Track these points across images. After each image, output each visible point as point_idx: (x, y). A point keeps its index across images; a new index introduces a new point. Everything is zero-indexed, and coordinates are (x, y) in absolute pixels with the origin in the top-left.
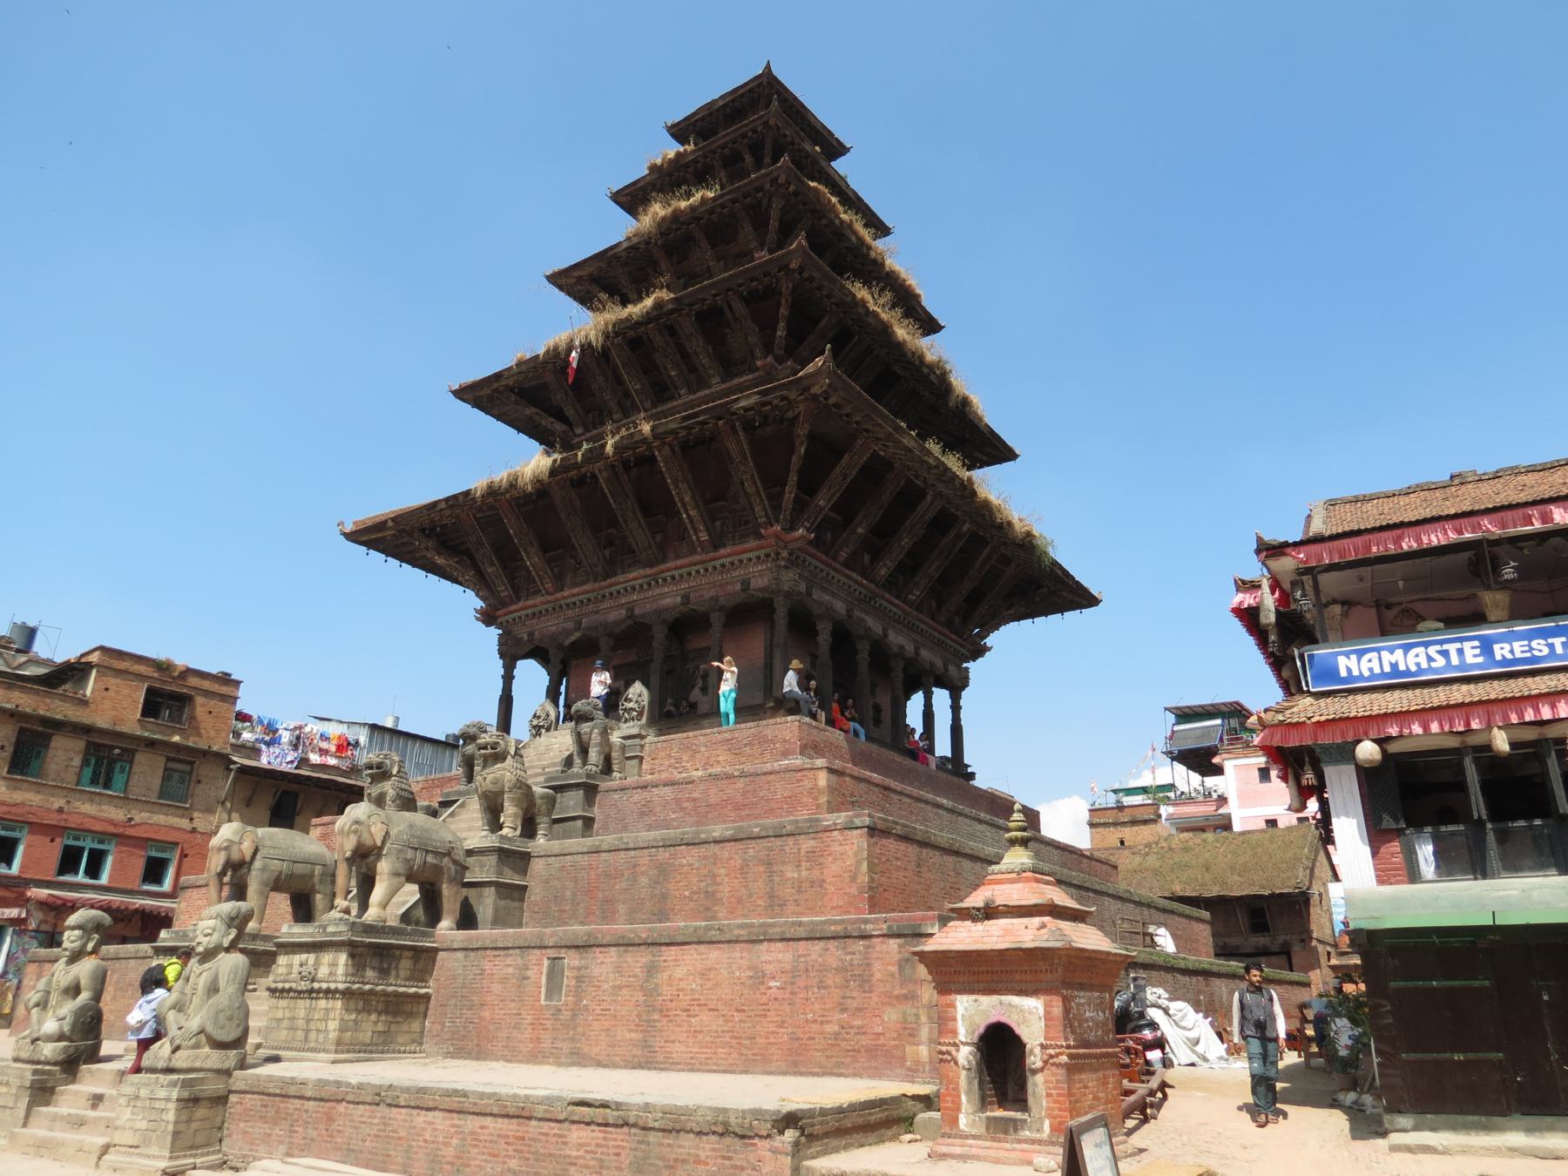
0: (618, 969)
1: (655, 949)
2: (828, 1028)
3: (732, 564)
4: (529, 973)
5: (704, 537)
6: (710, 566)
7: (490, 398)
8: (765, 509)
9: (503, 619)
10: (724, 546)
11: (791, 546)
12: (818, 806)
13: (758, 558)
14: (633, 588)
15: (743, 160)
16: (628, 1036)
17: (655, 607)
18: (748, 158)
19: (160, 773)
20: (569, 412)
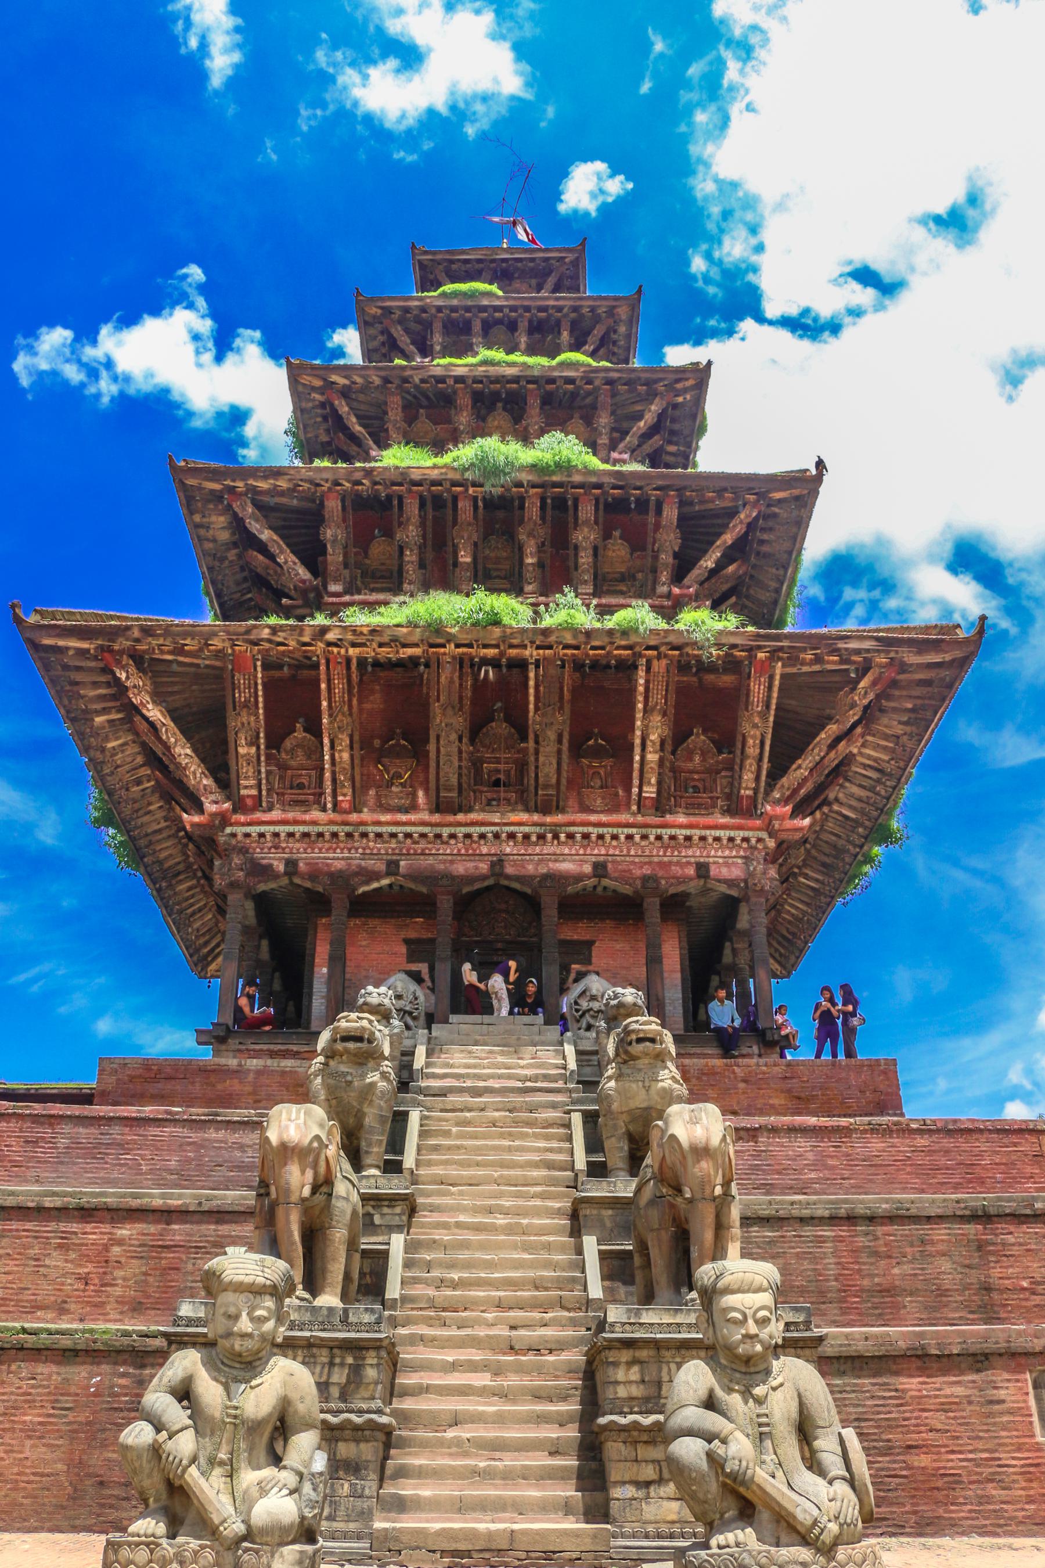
3: (688, 838)
4: (1002, 1394)
5: (650, 792)
6: (652, 833)
8: (757, 779)
11: (784, 836)
13: (731, 839)
14: (512, 836)
17: (545, 871)
18: (565, 335)
20: (334, 557)
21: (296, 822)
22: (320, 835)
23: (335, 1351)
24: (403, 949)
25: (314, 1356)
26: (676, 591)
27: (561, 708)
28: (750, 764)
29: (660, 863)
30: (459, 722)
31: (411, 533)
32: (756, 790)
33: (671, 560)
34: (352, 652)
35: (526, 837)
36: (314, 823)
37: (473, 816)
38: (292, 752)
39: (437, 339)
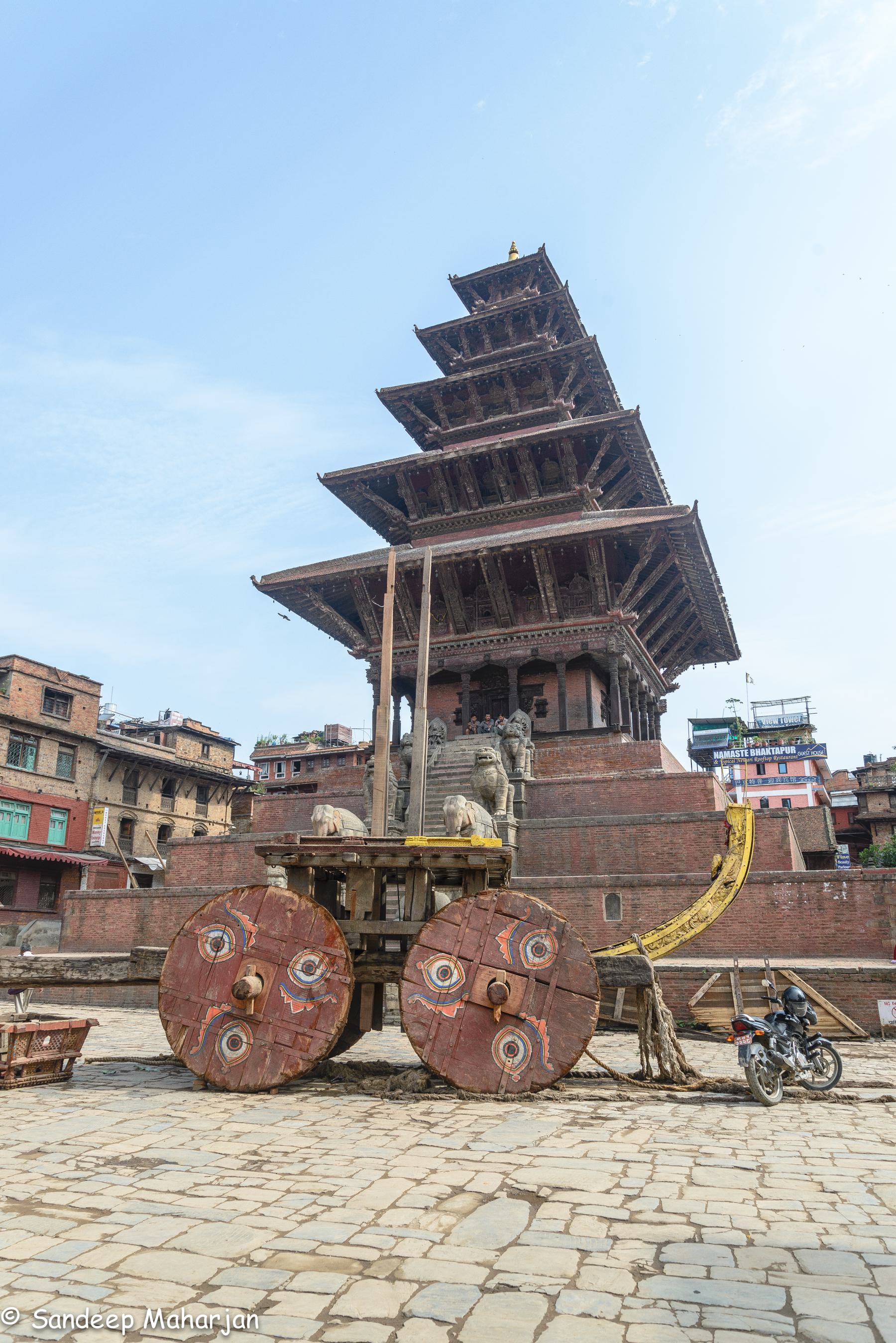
0: (664, 899)
1: (693, 888)
2: (827, 931)
3: (575, 631)
5: (554, 611)
6: (557, 632)
7: (345, 485)
8: (606, 596)
9: (373, 655)
10: (567, 618)
12: (708, 801)
14: (492, 641)
15: (529, 322)
17: (508, 656)
19: (56, 755)
20: (409, 502)
22: (408, 652)
26: (578, 488)
28: (601, 591)
29: (564, 645)
30: (456, 593)
31: (442, 484)
32: (607, 600)
33: (575, 470)
35: (498, 640)
37: (474, 634)
39: (465, 343)
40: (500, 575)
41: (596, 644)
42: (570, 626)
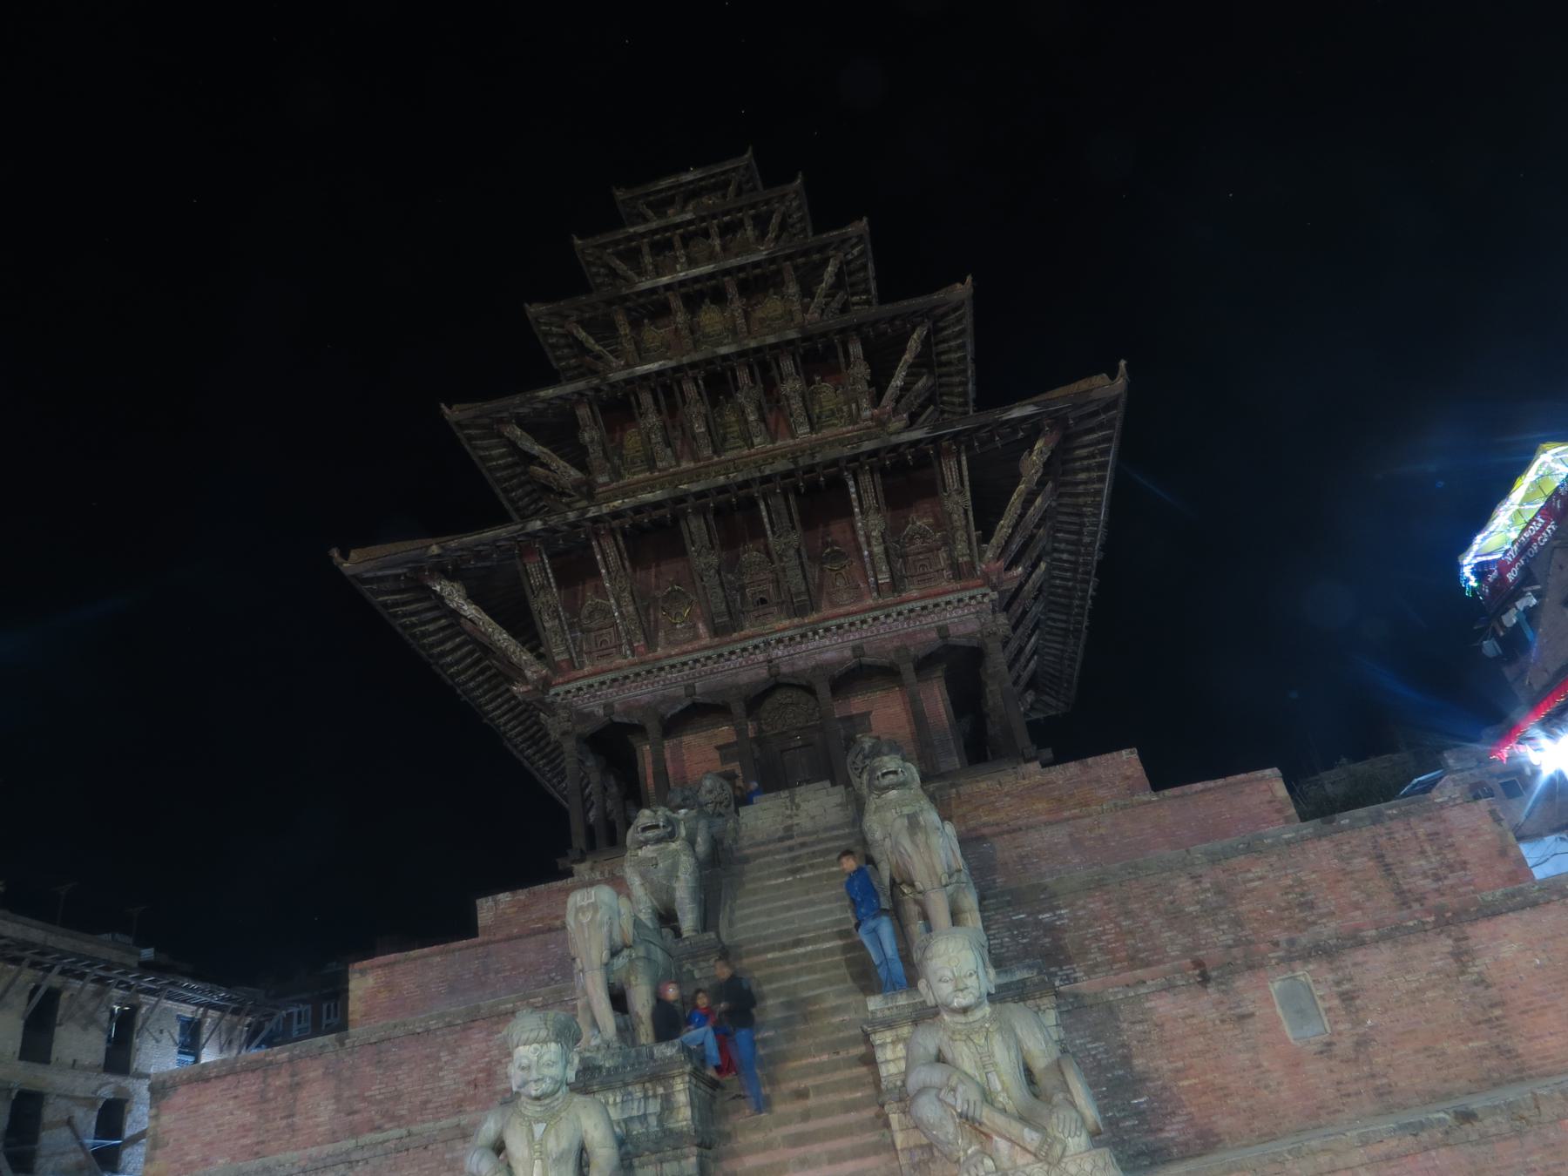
3: (924, 608)
4: (1251, 1008)
5: (884, 578)
6: (894, 611)
13: (960, 600)
14: (780, 641)
16: (1463, 1047)
20: (595, 453)
21: (604, 672)
22: (626, 677)
23: (648, 1085)
24: (716, 755)
25: (630, 1094)
27: (793, 528)
34: (615, 523)
35: (791, 639)
36: (618, 669)
38: (590, 616)
40: (791, 520)
41: (961, 628)
42: (915, 599)
